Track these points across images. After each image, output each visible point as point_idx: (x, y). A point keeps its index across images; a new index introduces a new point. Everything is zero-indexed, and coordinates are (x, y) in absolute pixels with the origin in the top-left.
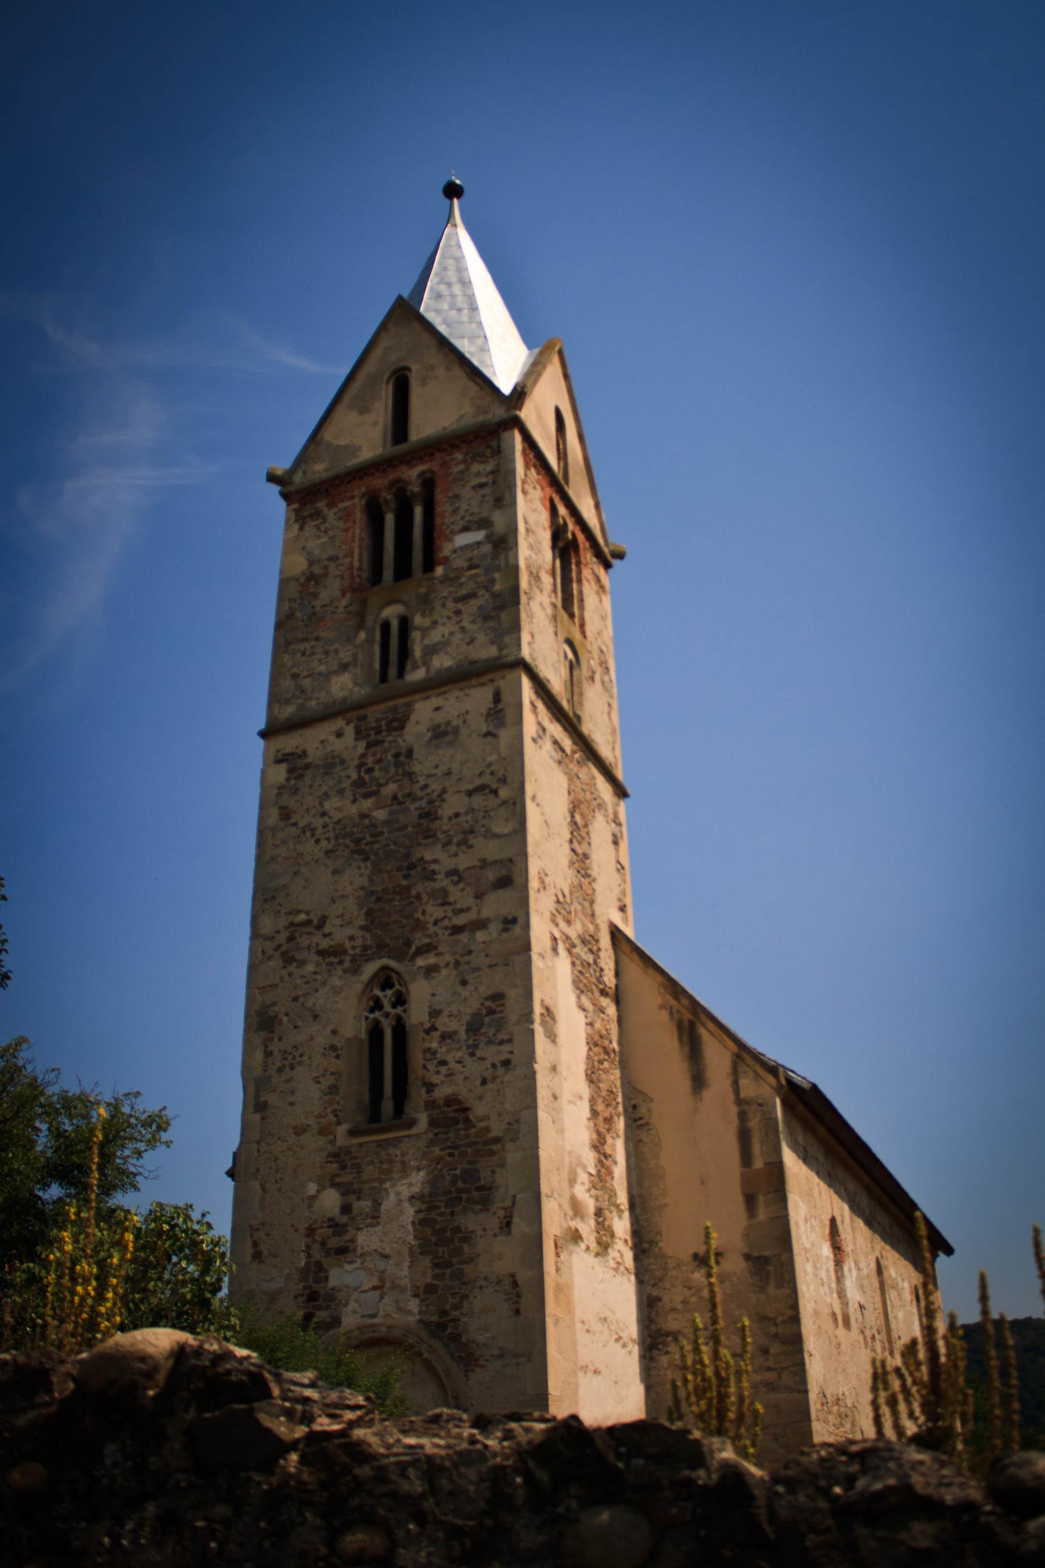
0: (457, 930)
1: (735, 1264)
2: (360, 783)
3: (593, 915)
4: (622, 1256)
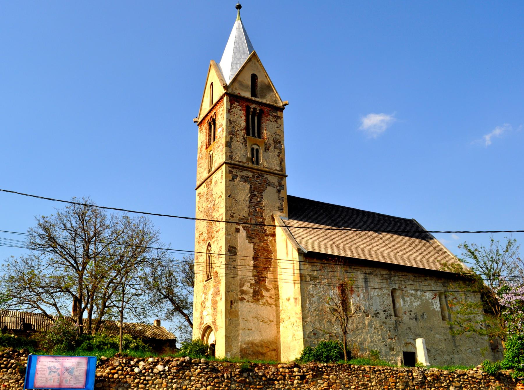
0: (217, 232)
1: (292, 300)
2: (207, 199)
3: (262, 217)
4: (267, 301)
